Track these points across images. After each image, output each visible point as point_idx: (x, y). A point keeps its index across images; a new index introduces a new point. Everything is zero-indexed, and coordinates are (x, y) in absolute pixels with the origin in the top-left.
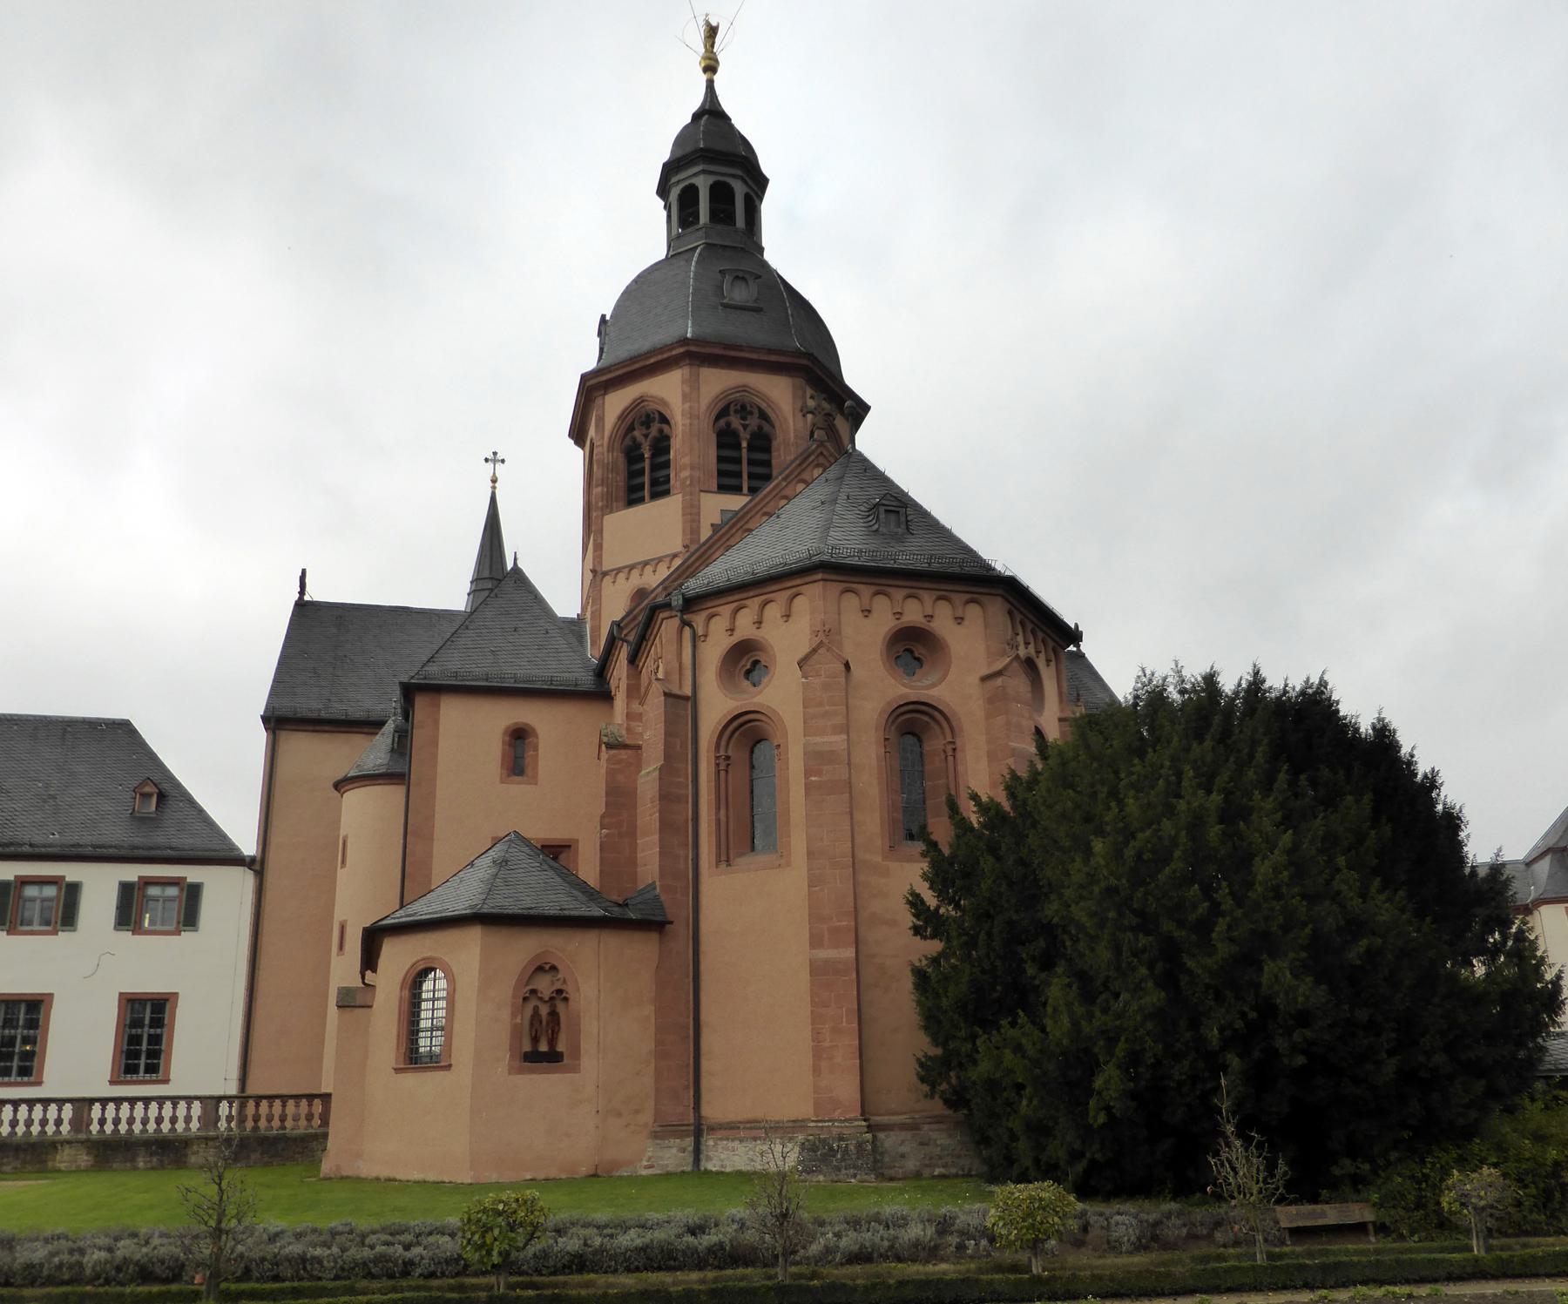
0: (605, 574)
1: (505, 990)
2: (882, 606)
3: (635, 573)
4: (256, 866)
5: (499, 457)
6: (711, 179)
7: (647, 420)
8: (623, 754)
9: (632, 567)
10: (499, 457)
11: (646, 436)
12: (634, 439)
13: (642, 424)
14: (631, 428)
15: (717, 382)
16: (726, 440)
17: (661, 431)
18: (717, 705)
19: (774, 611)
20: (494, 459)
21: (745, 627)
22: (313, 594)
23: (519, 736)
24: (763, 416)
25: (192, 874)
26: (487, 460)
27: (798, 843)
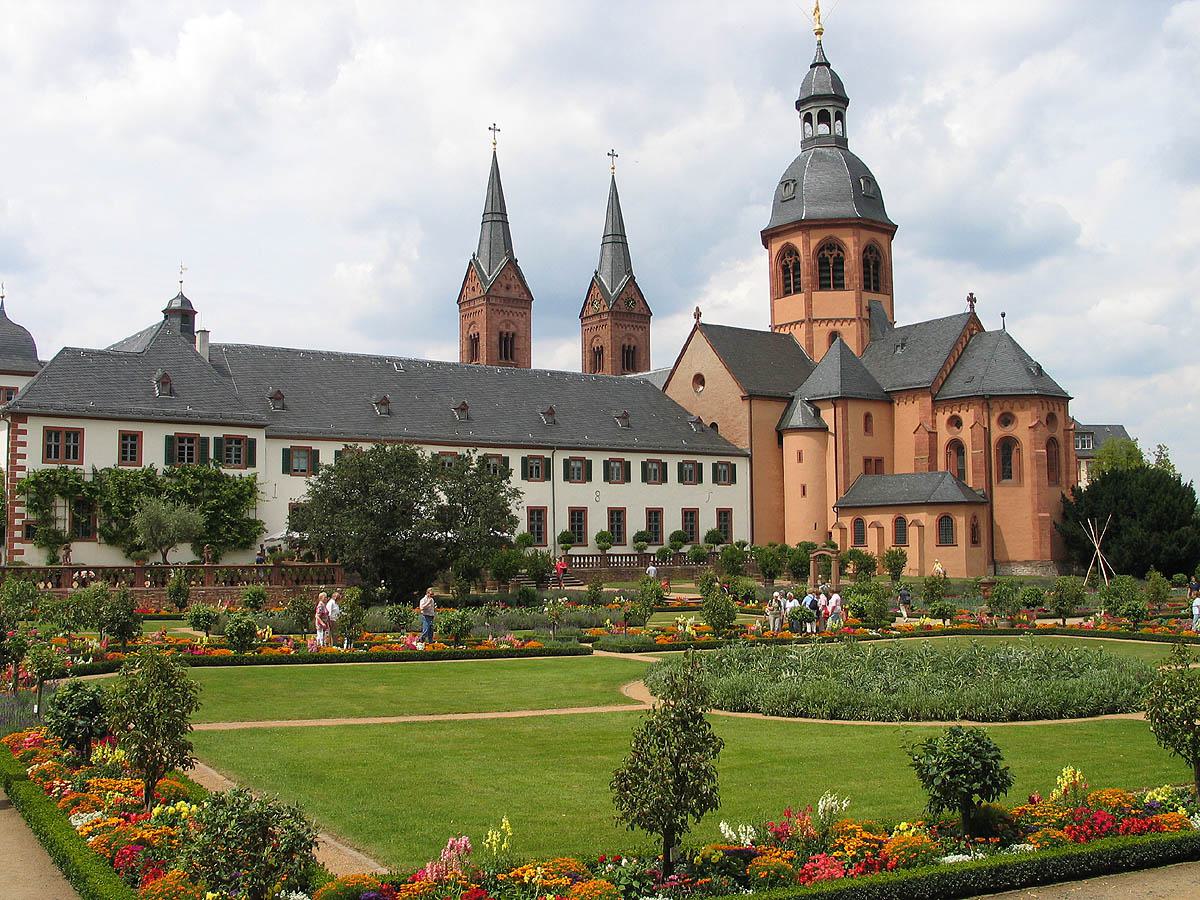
0: (816, 320)
1: (968, 524)
2: (1045, 405)
3: (831, 325)
4: (750, 457)
5: (497, 127)
6: (837, 109)
7: (831, 247)
8: (932, 435)
9: (830, 320)
10: (497, 127)
11: (831, 255)
12: (824, 255)
13: (828, 248)
14: (822, 249)
15: (866, 236)
16: (866, 263)
17: (838, 255)
18: (997, 433)
19: (1017, 405)
20: (494, 129)
21: (1007, 408)
22: (703, 320)
23: (868, 417)
24: (877, 253)
25: (732, 460)
26: (490, 129)
27: (1028, 480)
